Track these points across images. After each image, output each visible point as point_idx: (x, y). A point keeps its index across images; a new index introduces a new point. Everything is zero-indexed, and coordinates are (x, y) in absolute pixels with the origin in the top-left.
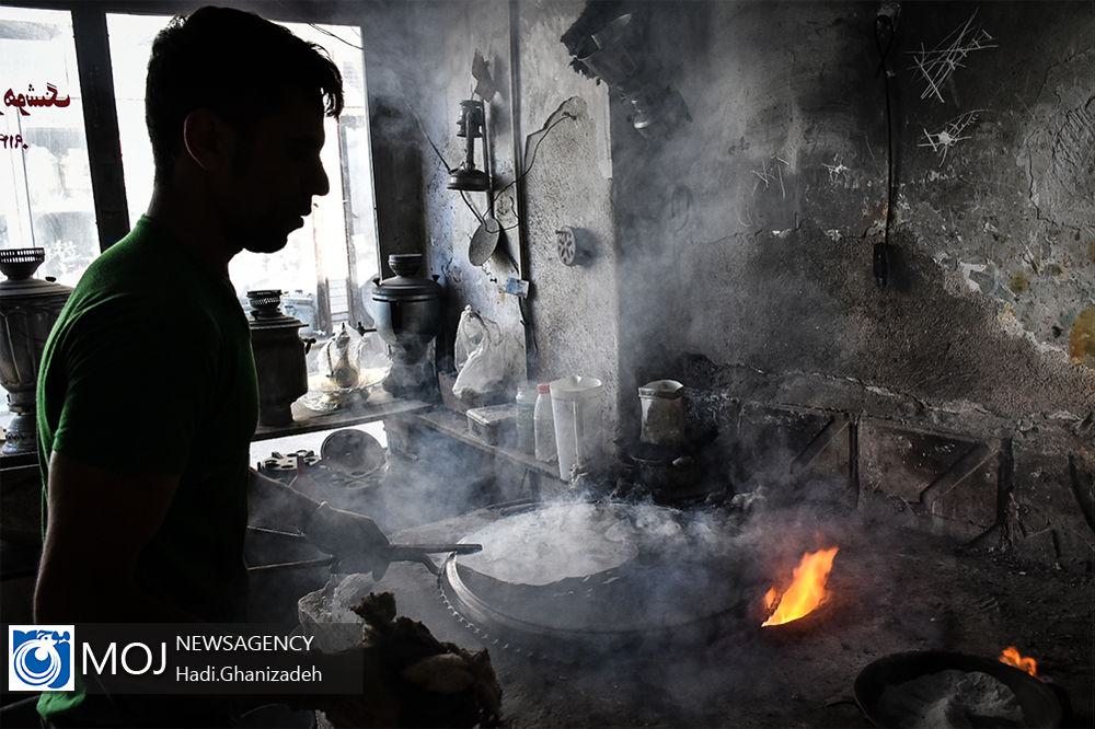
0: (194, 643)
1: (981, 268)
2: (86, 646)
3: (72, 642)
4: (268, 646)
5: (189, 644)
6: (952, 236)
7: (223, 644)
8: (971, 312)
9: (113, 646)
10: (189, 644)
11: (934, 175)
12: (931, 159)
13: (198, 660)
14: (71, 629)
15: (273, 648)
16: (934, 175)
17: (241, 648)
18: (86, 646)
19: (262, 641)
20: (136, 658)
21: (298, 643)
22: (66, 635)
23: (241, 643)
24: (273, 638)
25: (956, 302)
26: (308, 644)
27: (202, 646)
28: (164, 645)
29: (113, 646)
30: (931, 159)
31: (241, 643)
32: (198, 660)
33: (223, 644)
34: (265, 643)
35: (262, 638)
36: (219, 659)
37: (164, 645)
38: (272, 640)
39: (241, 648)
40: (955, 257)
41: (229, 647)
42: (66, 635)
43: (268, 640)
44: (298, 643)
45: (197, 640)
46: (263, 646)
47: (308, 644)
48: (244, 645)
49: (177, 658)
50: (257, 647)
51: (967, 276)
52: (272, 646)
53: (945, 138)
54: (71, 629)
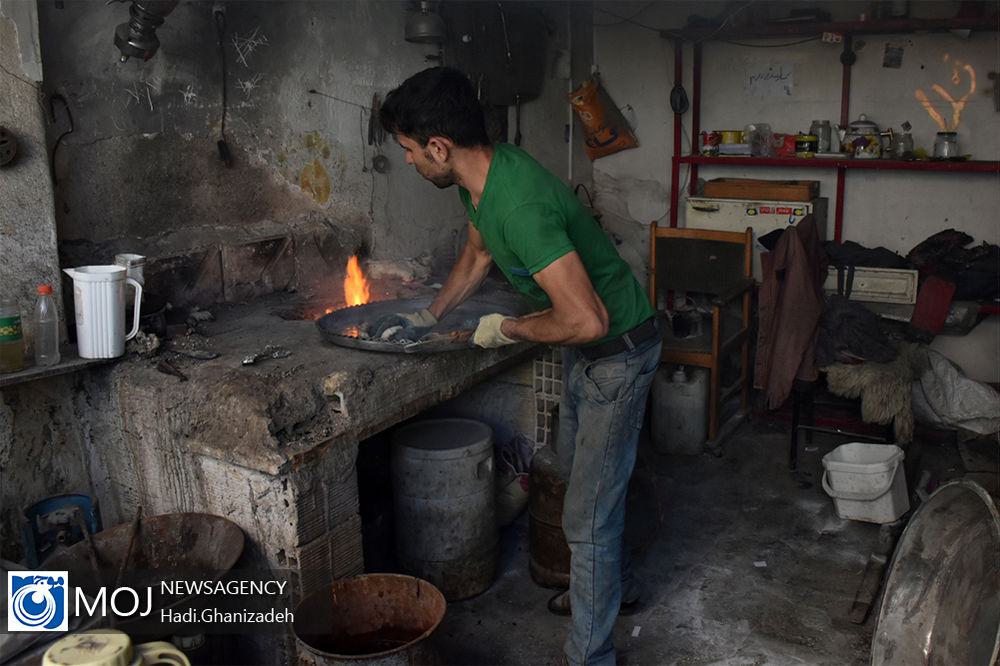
0: (177, 588)
1: (267, 152)
2: (79, 590)
3: (65, 586)
4: (244, 591)
5: (173, 588)
6: (253, 136)
7: (203, 589)
8: (259, 174)
9: (103, 590)
10: (173, 588)
11: (243, 104)
12: (243, 96)
13: (181, 603)
14: (65, 575)
16: (243, 104)
17: (220, 592)
20: (124, 601)
22: (61, 580)
23: (220, 587)
25: (256, 170)
26: (281, 588)
28: (149, 589)
29: (103, 590)
30: (243, 96)
31: (220, 587)
32: (181, 603)
33: (203, 589)
34: (242, 587)
35: (239, 583)
36: (201, 602)
37: (149, 589)
38: (248, 585)
39: (220, 592)
40: (255, 148)
41: (208, 591)
42: (61, 580)
43: (244, 585)
46: (240, 590)
47: (281, 588)
48: (223, 589)
49: (161, 601)
51: (258, 158)
52: (248, 590)
53: (248, 85)
54: (65, 575)
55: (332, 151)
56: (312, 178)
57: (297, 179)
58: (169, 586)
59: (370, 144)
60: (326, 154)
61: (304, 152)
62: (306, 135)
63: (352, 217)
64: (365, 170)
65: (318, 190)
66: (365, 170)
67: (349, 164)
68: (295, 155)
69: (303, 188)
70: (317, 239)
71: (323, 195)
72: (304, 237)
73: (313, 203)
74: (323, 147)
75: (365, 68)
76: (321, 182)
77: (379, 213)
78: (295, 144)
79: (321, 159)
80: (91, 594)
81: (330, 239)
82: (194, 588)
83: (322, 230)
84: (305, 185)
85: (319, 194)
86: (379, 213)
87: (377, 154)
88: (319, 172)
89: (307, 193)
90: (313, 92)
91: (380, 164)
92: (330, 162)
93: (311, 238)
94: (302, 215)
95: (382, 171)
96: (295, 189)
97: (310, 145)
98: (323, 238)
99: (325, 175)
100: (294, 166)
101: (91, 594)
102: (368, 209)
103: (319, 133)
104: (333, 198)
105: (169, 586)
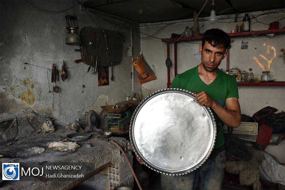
0: (51, 168)
2: (22, 168)
3: (19, 167)
5: (49, 168)
7: (58, 168)
9: (29, 168)
13: (52, 172)
14: (18, 164)
17: (63, 169)
18: (22, 168)
19: (68, 167)
20: (35, 172)
22: (17, 165)
24: (71, 166)
26: (80, 168)
27: (53, 168)
28: (43, 168)
29: (29, 168)
32: (52, 172)
33: (58, 168)
35: (68, 166)
37: (43, 168)
39: (63, 169)
41: (60, 169)
42: (17, 165)
43: (70, 167)
47: (80, 168)
50: (67, 169)
54: (18, 164)
55: (35, 86)
56: (26, 96)
57: (19, 96)
59: (52, 82)
60: (33, 86)
61: (23, 86)
62: (23, 80)
63: (44, 109)
64: (50, 92)
65: (29, 100)
66: (50, 92)
67: (43, 90)
68: (18, 88)
69: (22, 100)
70: (28, 119)
71: (31, 102)
72: (22, 119)
73: (27, 105)
74: (31, 84)
75: (49, 54)
76: (30, 97)
77: (57, 107)
78: (18, 83)
79: (30, 89)
80: (26, 170)
81: (34, 118)
83: (30, 115)
84: (23, 99)
85: (30, 102)
86: (57, 107)
87: (55, 86)
88: (29, 93)
89: (24, 102)
90: (26, 63)
91: (57, 89)
92: (34, 89)
93: (26, 118)
94: (22, 110)
95: (57, 92)
96: (19, 101)
97: (25, 83)
98: (31, 118)
99: (32, 94)
100: (18, 92)
101: (26, 170)
102: (51, 106)
103: (30, 79)
104: (36, 102)
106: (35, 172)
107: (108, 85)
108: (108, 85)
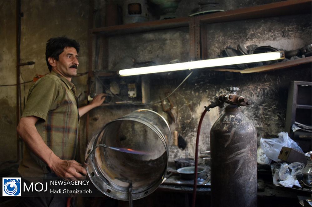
0: (55, 183)
2: (25, 183)
3: (20, 182)
4: (76, 184)
5: (54, 183)
7: (63, 183)
9: (32, 183)
10: (54, 183)
13: (57, 187)
14: (20, 179)
15: (78, 184)
18: (25, 183)
20: (39, 187)
21: (85, 183)
22: (19, 180)
23: (69, 183)
24: (78, 181)
26: (88, 183)
28: (47, 183)
29: (32, 183)
31: (69, 183)
32: (57, 187)
33: (63, 183)
34: (76, 183)
35: (75, 181)
36: (62, 187)
37: (47, 183)
38: (77, 182)
41: (65, 184)
42: (19, 180)
44: (85, 183)
45: (56, 182)
46: (75, 183)
47: (88, 183)
49: (50, 187)
50: (73, 184)
52: (77, 184)
54: (20, 179)
58: (53, 182)
80: (28, 185)
82: (61, 183)
101: (28, 185)
105: (53, 182)
106: (39, 187)
107: (278, 158)
108: (278, 158)
